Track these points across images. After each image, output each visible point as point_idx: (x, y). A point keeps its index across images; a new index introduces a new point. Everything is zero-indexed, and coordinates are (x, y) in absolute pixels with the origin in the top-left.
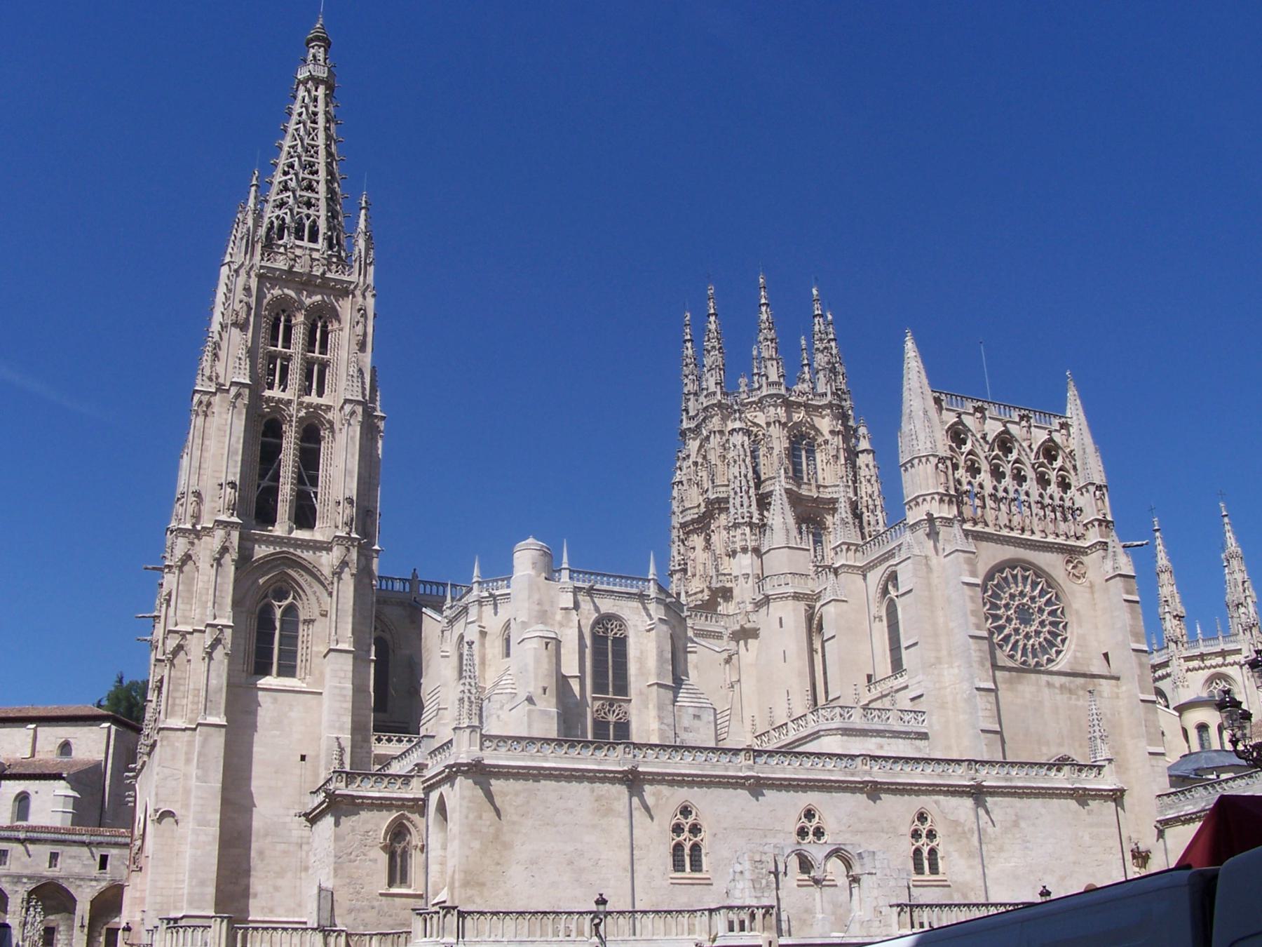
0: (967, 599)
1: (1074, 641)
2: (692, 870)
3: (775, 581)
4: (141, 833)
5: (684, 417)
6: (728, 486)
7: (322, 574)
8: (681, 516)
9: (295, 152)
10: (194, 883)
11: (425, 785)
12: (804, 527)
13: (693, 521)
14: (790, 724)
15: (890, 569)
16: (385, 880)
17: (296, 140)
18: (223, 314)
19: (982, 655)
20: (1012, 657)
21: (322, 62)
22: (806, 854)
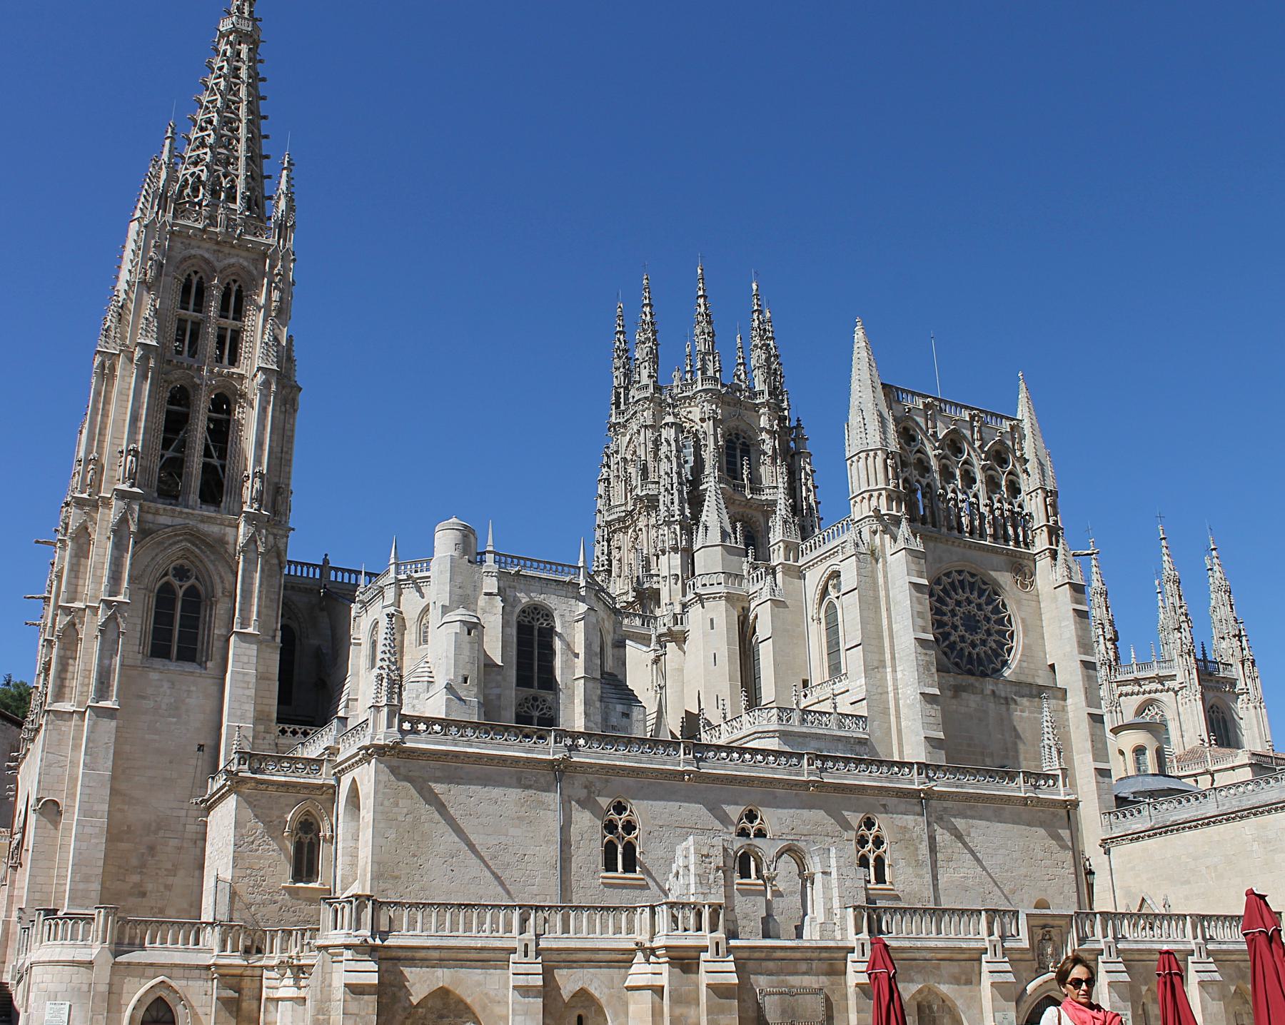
0: (914, 599)
1: (1020, 652)
2: (626, 870)
3: (706, 580)
4: (21, 825)
5: (614, 412)
6: (658, 483)
7: (226, 552)
8: (606, 514)
9: (213, 107)
10: (77, 879)
11: (336, 770)
12: (738, 525)
13: (619, 520)
14: (723, 726)
15: (830, 569)
16: (289, 870)
17: (215, 95)
18: (130, 271)
19: (928, 658)
20: (957, 664)
21: (246, 15)
22: (757, 849)
